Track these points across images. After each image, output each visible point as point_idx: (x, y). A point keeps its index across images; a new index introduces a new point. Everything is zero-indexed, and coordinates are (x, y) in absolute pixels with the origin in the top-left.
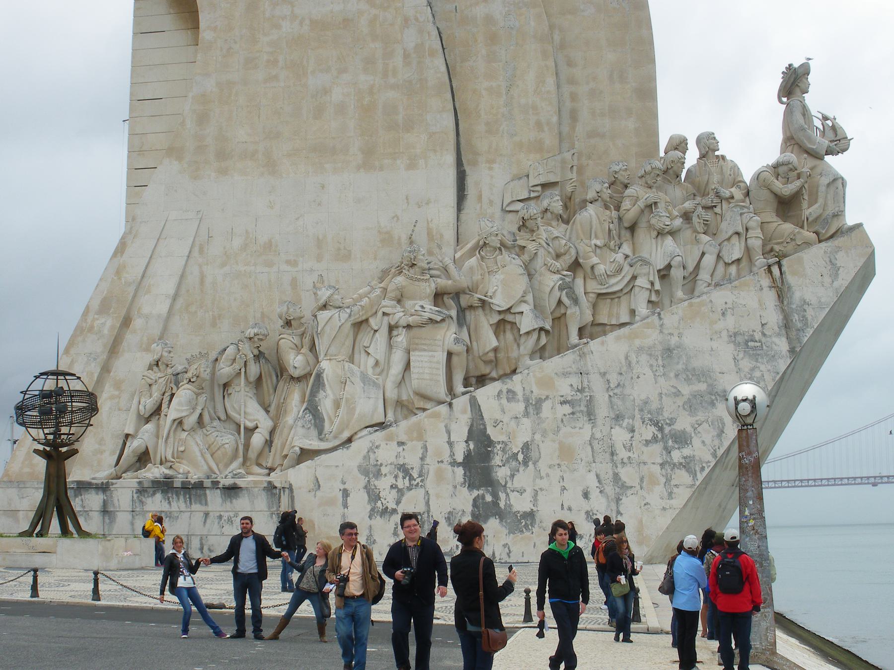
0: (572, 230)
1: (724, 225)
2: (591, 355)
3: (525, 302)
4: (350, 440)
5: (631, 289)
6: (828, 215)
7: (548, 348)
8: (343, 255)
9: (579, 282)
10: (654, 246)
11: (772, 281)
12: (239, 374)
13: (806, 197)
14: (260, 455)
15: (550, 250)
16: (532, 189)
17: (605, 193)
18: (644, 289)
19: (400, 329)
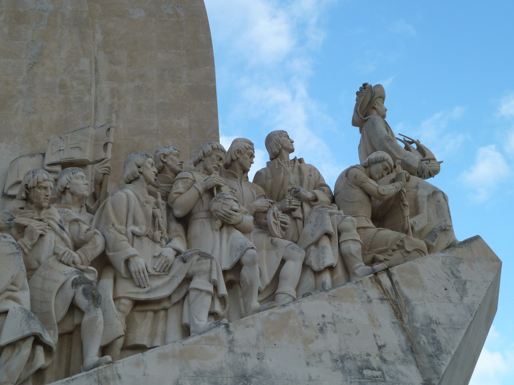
0: (100, 217)
1: (308, 228)
2: (118, 381)
3: (15, 300)
5: (184, 298)
6: (434, 228)
9: (107, 283)
11: (382, 291)
13: (407, 203)
15: (65, 235)
16: (48, 168)
18: (203, 294)
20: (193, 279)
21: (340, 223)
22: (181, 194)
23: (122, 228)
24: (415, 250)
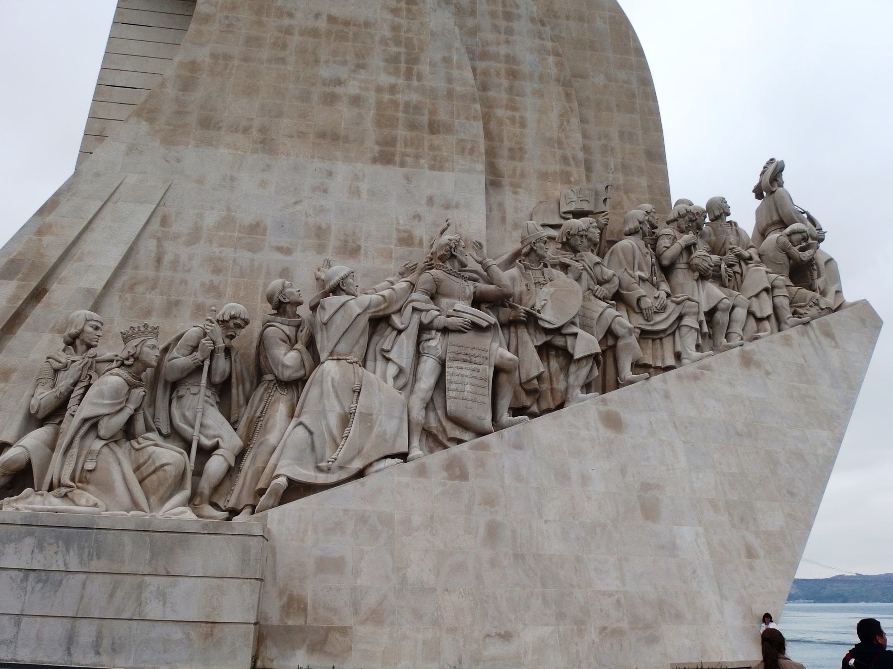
3: (573, 323)
4: (361, 474)
7: (593, 383)
8: (350, 249)
10: (697, 288)
12: (199, 369)
14: (216, 489)
16: (563, 215)
17: (646, 225)
18: (693, 330)
19: (434, 332)
20: (684, 318)
21: (774, 281)
22: (668, 248)
23: (631, 272)
24: (826, 308)
